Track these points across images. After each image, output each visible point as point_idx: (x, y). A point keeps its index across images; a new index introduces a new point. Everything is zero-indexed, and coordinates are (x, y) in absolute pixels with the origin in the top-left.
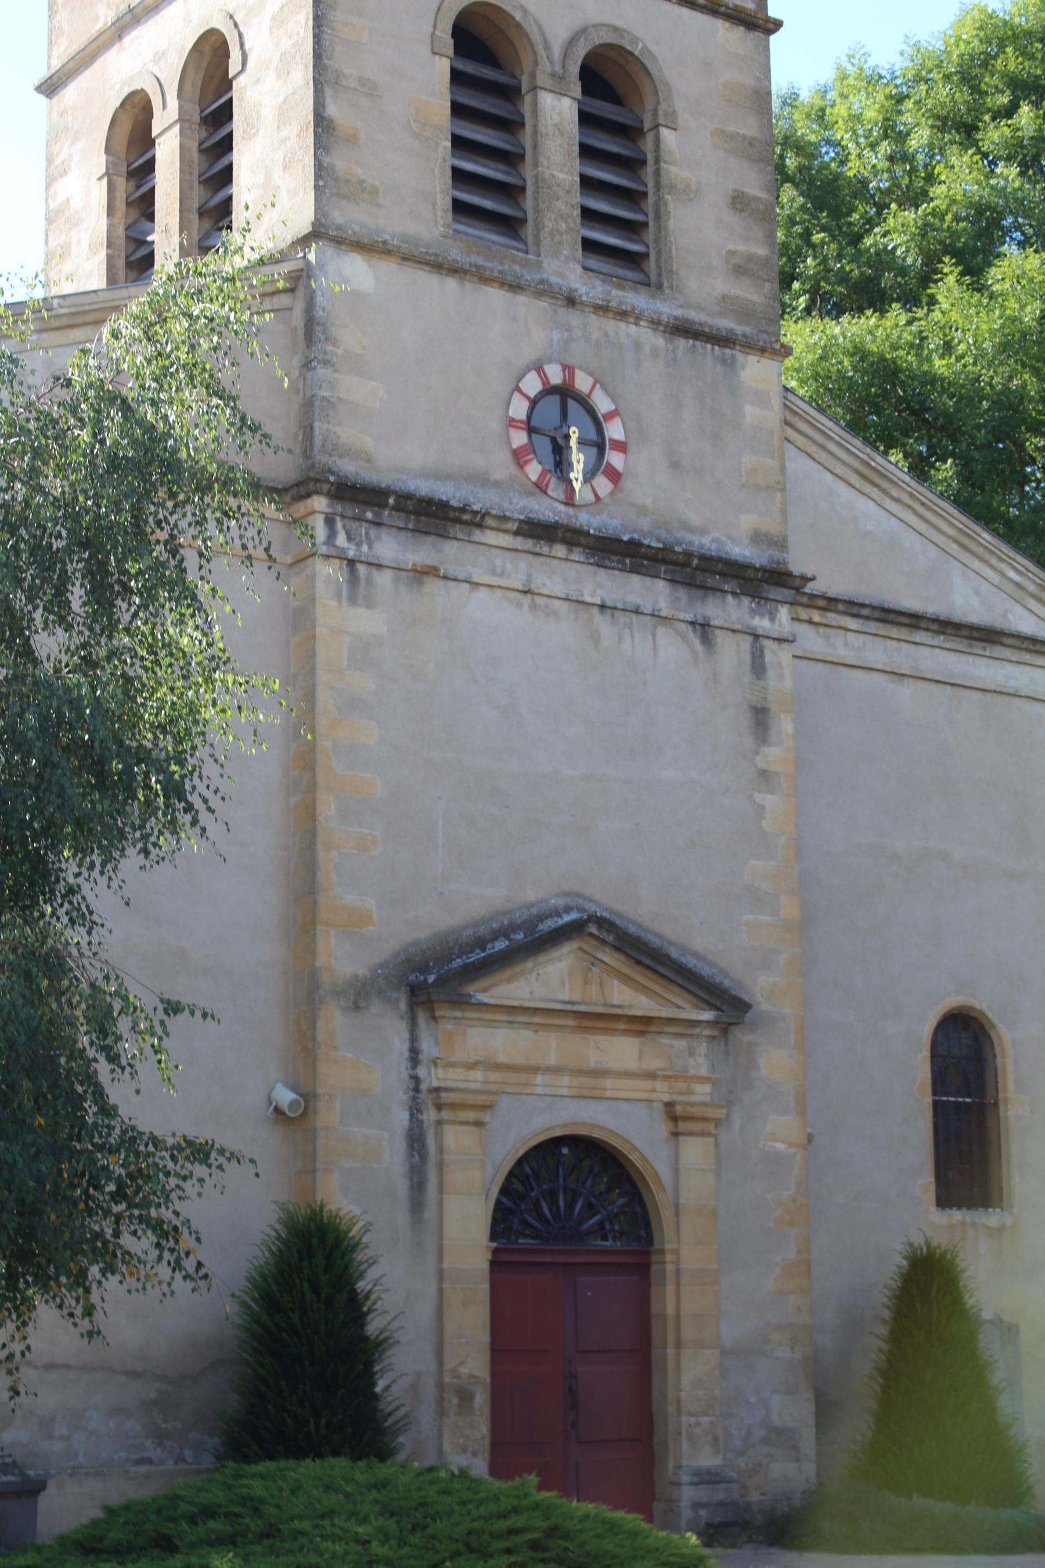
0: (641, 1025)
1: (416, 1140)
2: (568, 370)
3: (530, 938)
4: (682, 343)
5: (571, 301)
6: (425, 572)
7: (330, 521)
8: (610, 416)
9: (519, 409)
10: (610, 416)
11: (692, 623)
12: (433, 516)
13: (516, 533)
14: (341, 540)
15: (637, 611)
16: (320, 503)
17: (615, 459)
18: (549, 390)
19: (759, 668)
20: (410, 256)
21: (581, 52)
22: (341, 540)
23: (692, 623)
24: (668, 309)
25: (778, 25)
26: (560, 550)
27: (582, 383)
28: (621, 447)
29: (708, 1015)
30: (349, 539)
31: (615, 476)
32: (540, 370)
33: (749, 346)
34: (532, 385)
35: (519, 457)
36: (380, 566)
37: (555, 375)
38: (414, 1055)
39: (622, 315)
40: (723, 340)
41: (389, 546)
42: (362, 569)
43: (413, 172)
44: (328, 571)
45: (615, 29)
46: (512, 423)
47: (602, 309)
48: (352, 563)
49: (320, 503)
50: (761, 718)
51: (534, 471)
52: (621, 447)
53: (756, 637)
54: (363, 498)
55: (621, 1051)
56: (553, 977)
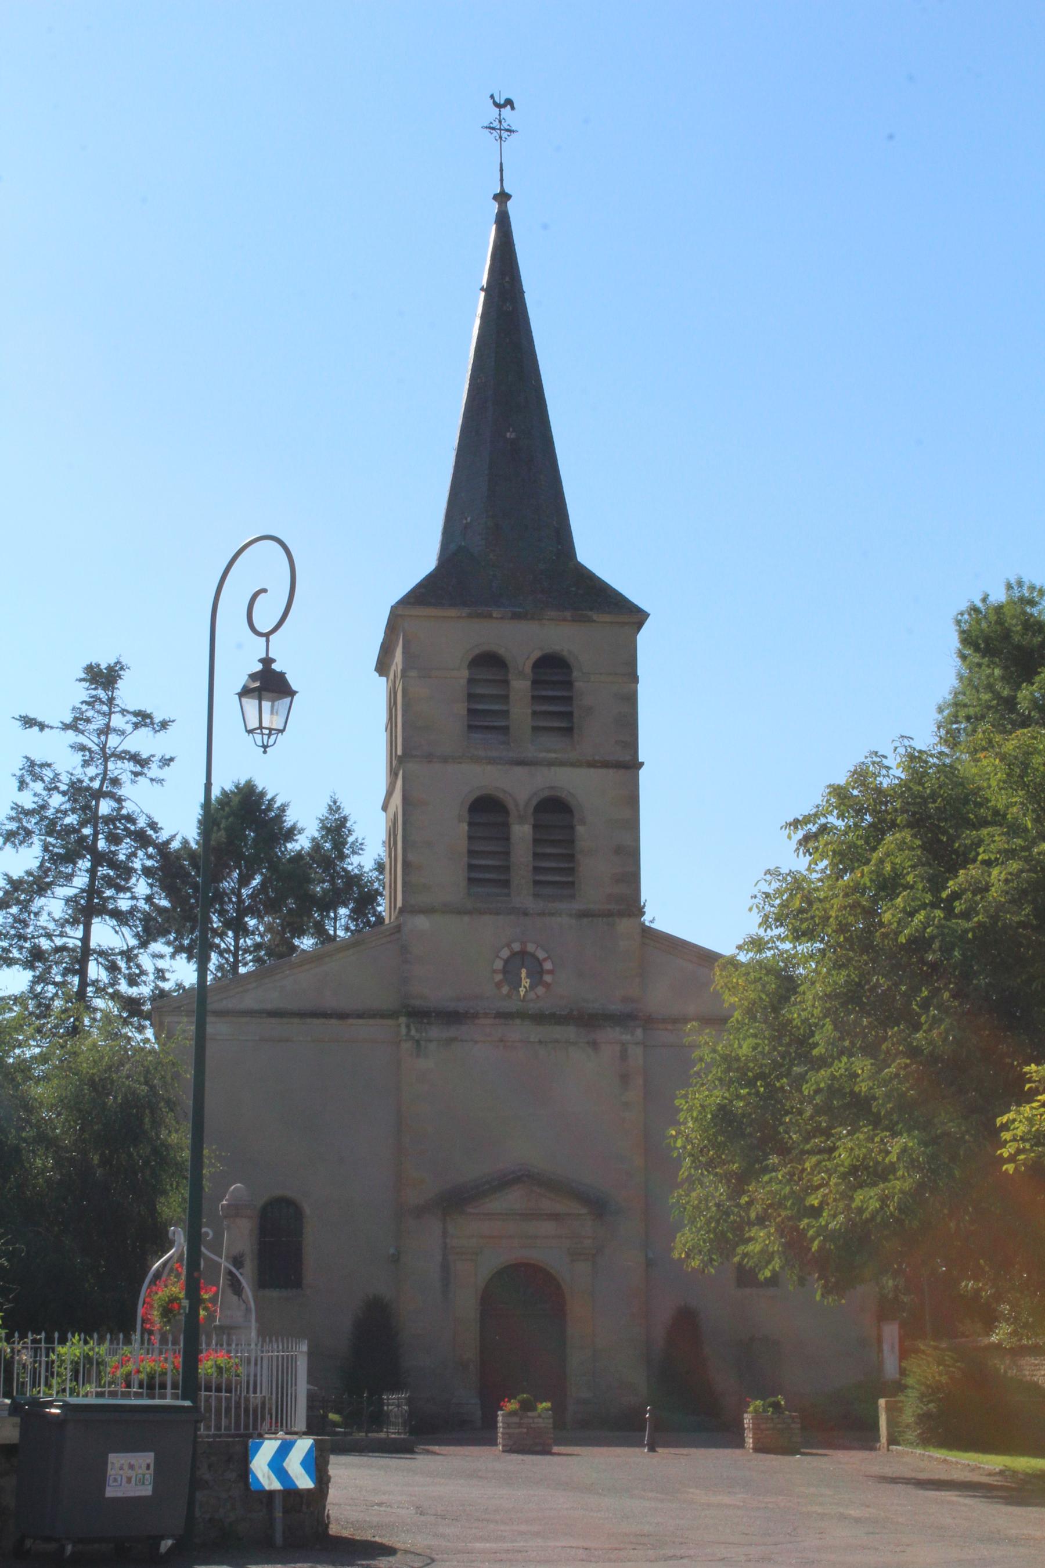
0: (555, 1217)
1: (445, 1268)
2: (524, 944)
3: (504, 1182)
4: (585, 920)
5: (526, 914)
6: (450, 1041)
7: (408, 1027)
8: (545, 960)
9: (499, 965)
10: (545, 960)
11: (588, 1043)
12: (452, 1017)
13: (495, 1018)
14: (413, 1032)
15: (557, 1041)
16: (403, 1020)
17: (548, 978)
18: (514, 954)
19: (624, 1056)
20: (447, 909)
21: (534, 802)
22: (413, 1032)
23: (588, 1043)
24: (577, 906)
25: (642, 764)
26: (518, 1021)
27: (531, 948)
28: (551, 972)
29: (584, 1211)
30: (417, 1030)
31: (547, 986)
32: (508, 945)
33: (621, 914)
34: (505, 953)
35: (498, 985)
36: (431, 1041)
37: (516, 947)
38: (445, 1234)
39: (552, 914)
40: (609, 914)
41: (435, 1032)
42: (423, 1043)
43: (448, 877)
44: (406, 1046)
45: (552, 788)
46: (495, 971)
47: (542, 914)
48: (418, 1042)
49: (403, 1020)
50: (625, 1079)
51: (505, 990)
52: (551, 972)
53: (623, 1044)
54: (420, 1015)
55: (548, 1228)
56: (513, 1199)
